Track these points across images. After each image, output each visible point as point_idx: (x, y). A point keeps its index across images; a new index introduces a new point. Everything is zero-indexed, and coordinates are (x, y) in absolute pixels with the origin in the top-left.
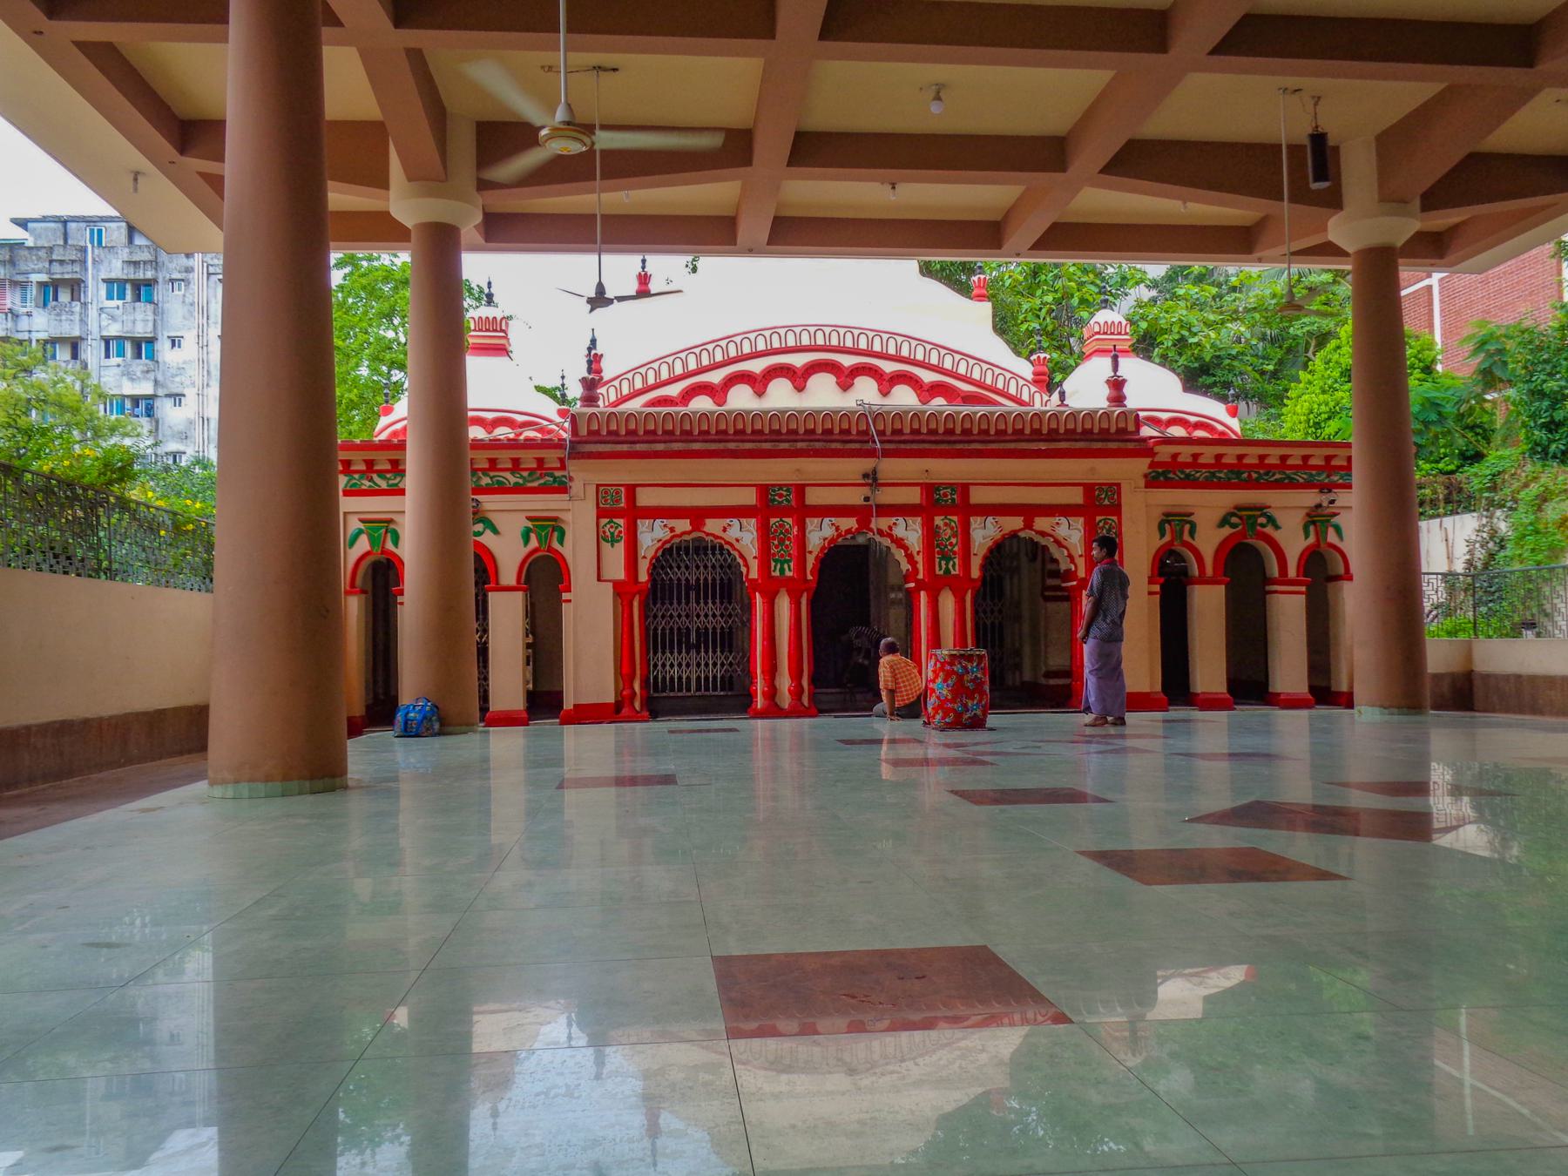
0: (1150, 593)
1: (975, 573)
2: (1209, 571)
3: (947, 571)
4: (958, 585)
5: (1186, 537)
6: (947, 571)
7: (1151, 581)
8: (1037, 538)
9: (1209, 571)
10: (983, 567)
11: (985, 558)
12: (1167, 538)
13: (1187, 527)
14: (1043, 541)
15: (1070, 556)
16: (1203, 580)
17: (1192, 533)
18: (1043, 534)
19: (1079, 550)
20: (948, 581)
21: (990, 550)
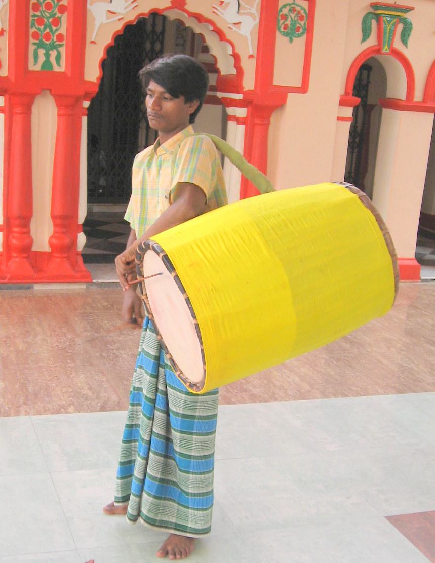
0: (340, 119)
1: (93, 73)
2: (418, 96)
3: (47, 63)
4: (64, 90)
5: (398, 45)
6: (47, 63)
7: (343, 103)
8: (190, 23)
9: (418, 96)
10: (103, 64)
11: (110, 50)
12: (372, 41)
13: (400, 27)
14: (198, 29)
15: (236, 56)
16: (408, 106)
17: (404, 38)
18: (199, 18)
19: (248, 45)
20: (47, 82)
21: (118, 38)
